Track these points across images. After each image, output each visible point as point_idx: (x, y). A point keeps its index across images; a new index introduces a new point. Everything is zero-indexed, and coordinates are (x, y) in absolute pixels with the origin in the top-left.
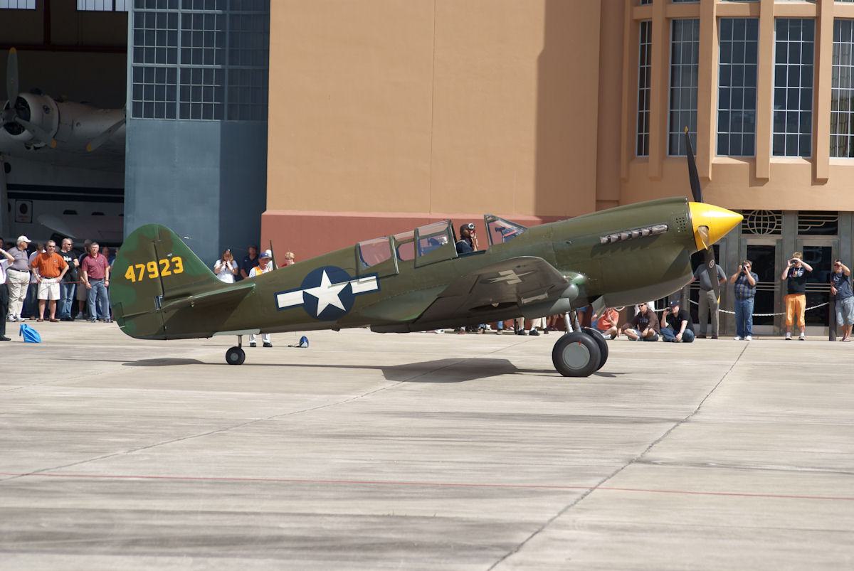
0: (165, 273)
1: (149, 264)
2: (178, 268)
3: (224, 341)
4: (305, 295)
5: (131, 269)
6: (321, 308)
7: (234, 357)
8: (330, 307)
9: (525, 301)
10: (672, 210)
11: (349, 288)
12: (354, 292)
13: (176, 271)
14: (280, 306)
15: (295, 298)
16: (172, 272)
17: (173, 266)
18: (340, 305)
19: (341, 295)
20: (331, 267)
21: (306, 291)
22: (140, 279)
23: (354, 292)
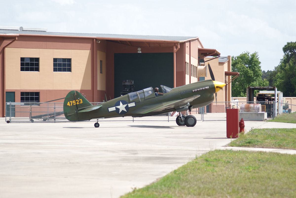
0: (77, 103)
1: (73, 101)
2: (81, 102)
3: (94, 121)
4: (116, 107)
5: (69, 103)
6: (120, 111)
7: (97, 125)
8: (123, 111)
10: (210, 83)
11: (127, 106)
14: (110, 111)
15: (113, 109)
17: (80, 101)
18: (125, 110)
19: (126, 108)
20: (123, 101)
21: (116, 107)
22: (71, 105)
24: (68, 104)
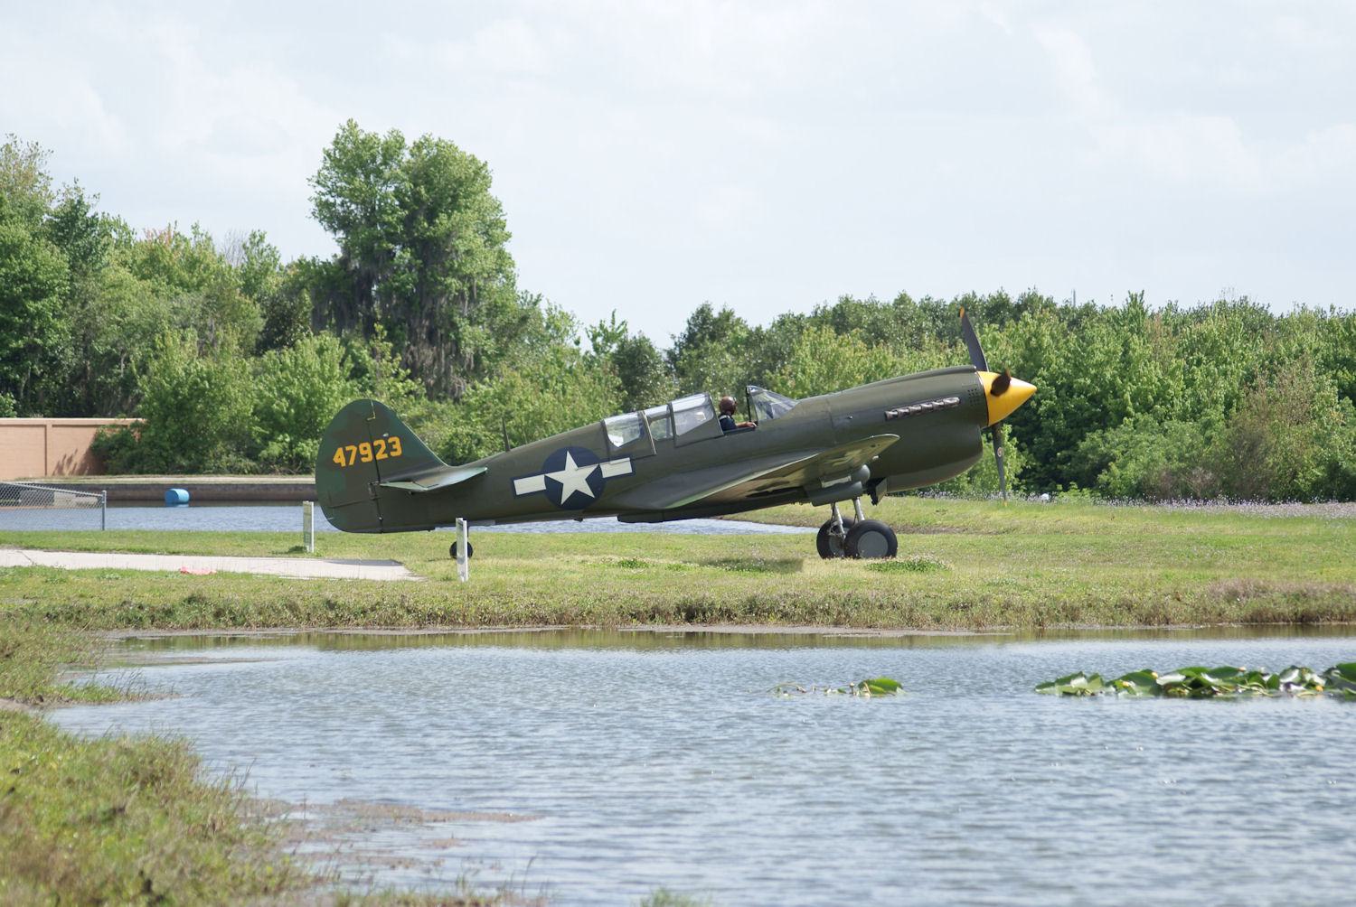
0: (380, 456)
1: (362, 446)
2: (396, 450)
4: (548, 480)
5: (340, 452)
6: (566, 495)
8: (577, 494)
9: (826, 485)
10: (962, 382)
11: (598, 471)
13: (393, 454)
14: (519, 492)
16: (389, 455)
17: (389, 448)
18: (589, 492)
19: (589, 480)
21: (549, 475)
22: (351, 463)
24: (339, 457)
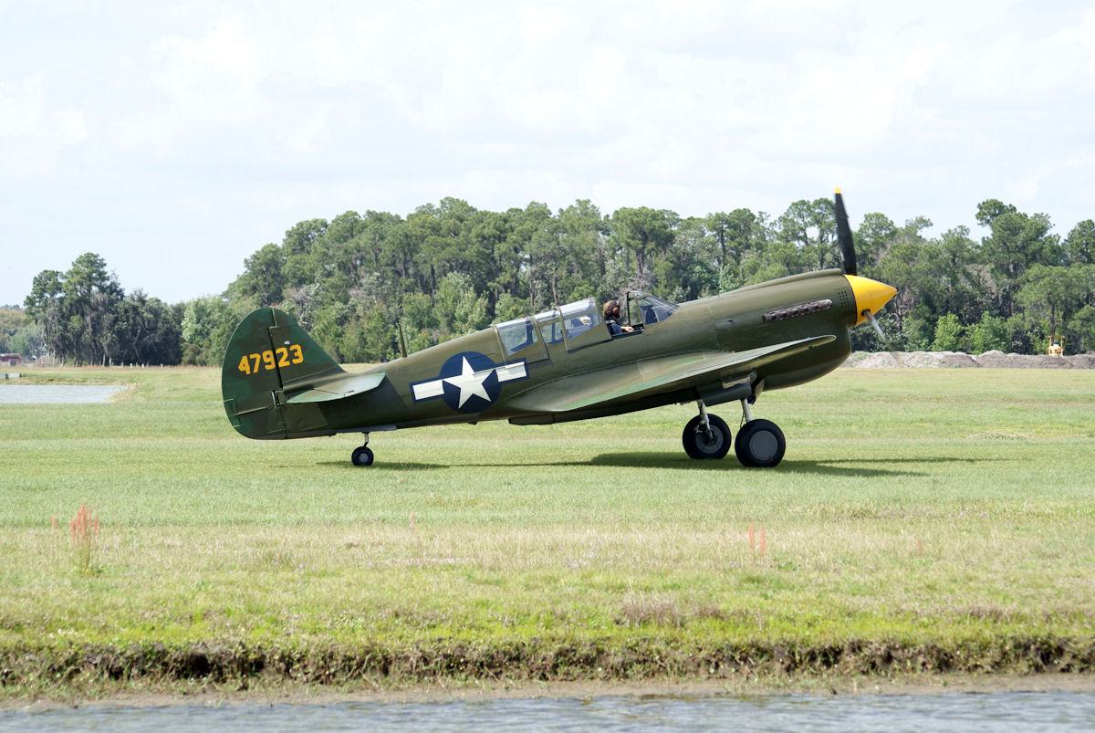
0: (282, 363)
1: (265, 354)
2: (297, 357)
5: (244, 360)
6: (463, 399)
7: (364, 457)
8: (474, 397)
9: (726, 385)
11: (494, 375)
12: (500, 381)
13: (295, 361)
14: (417, 398)
17: (291, 356)
18: (485, 396)
22: (256, 370)
23: (500, 381)
